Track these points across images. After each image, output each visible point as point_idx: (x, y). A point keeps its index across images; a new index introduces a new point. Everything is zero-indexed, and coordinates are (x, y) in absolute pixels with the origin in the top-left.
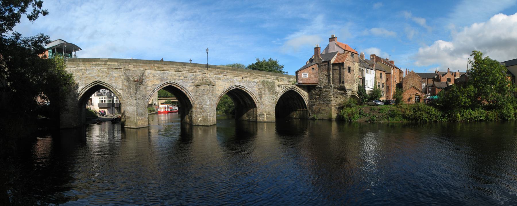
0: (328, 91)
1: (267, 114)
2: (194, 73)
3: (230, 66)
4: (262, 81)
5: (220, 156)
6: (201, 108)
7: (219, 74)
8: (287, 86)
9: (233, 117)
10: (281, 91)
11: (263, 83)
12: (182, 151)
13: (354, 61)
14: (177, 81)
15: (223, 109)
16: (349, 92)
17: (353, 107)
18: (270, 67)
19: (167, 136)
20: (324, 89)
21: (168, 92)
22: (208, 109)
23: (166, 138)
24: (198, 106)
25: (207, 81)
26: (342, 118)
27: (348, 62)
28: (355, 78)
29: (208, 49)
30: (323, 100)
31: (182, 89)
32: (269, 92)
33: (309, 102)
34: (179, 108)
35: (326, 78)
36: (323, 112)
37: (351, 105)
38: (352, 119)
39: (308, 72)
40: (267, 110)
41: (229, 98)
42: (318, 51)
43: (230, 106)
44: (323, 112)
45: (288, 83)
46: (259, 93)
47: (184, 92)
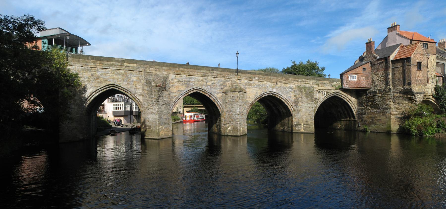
0: (385, 96)
1: (304, 124)
3: (263, 71)
4: (299, 87)
5: (251, 169)
6: (231, 116)
7: (250, 80)
8: (328, 91)
9: (265, 127)
10: (321, 98)
11: (300, 88)
12: (209, 163)
13: (429, 53)
14: (204, 88)
15: (255, 117)
16: (418, 97)
17: (427, 117)
18: (308, 70)
19: (193, 147)
20: (379, 94)
21: (194, 99)
22: (238, 118)
23: (192, 149)
24: (227, 115)
25: (237, 87)
26: (406, 131)
27: (418, 55)
28: (429, 76)
29: (238, 52)
30: (378, 107)
31: (210, 96)
32: (307, 99)
33: (358, 110)
34: (206, 116)
35: (382, 79)
36: (378, 123)
37: (422, 114)
38: (424, 133)
39: (356, 74)
40: (305, 120)
41: (261, 105)
42: (371, 46)
43: (262, 115)
44: (378, 123)
45: (330, 88)
46: (295, 100)
47: (212, 99)
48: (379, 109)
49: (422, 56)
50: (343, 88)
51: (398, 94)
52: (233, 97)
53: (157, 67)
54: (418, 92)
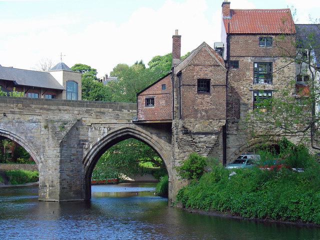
45: (115, 121)
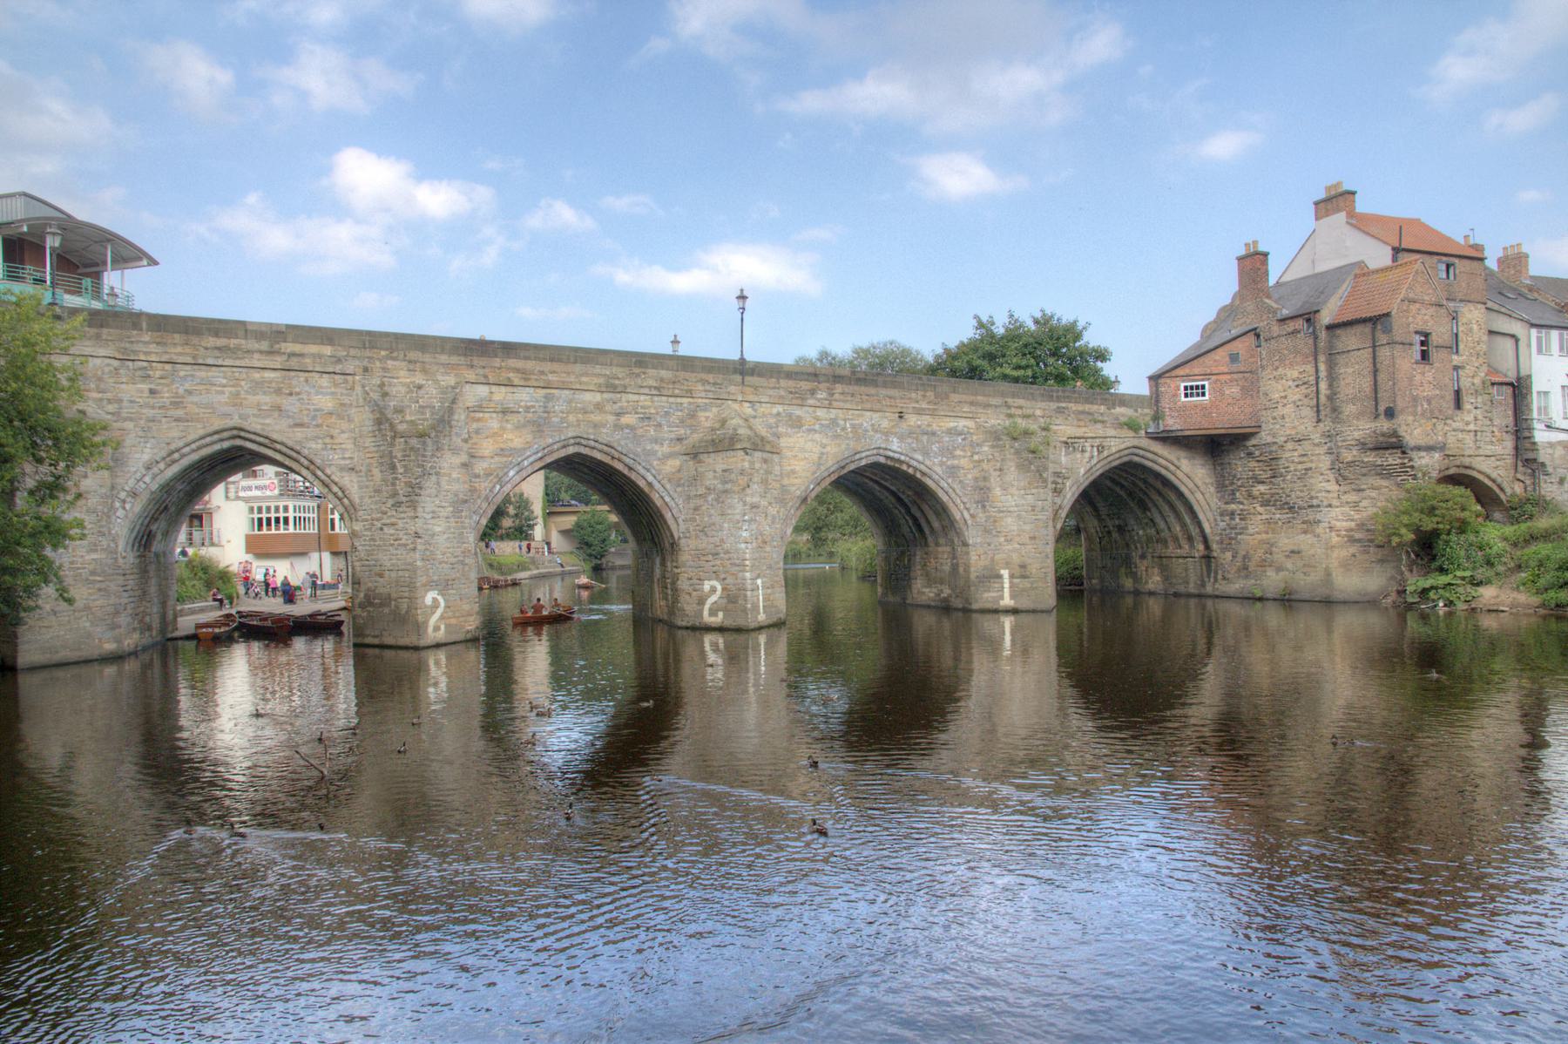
0: (1312, 461)
2: (685, 400)
7: (795, 401)
10: (1081, 468)
14: (605, 435)
27: (1417, 305)
29: (745, 293)
47: (642, 484)
48: (1291, 508)
49: (1432, 310)
50: (1161, 429)
51: (1355, 452)
52: (724, 471)
53: (412, 355)
54: (1422, 443)
